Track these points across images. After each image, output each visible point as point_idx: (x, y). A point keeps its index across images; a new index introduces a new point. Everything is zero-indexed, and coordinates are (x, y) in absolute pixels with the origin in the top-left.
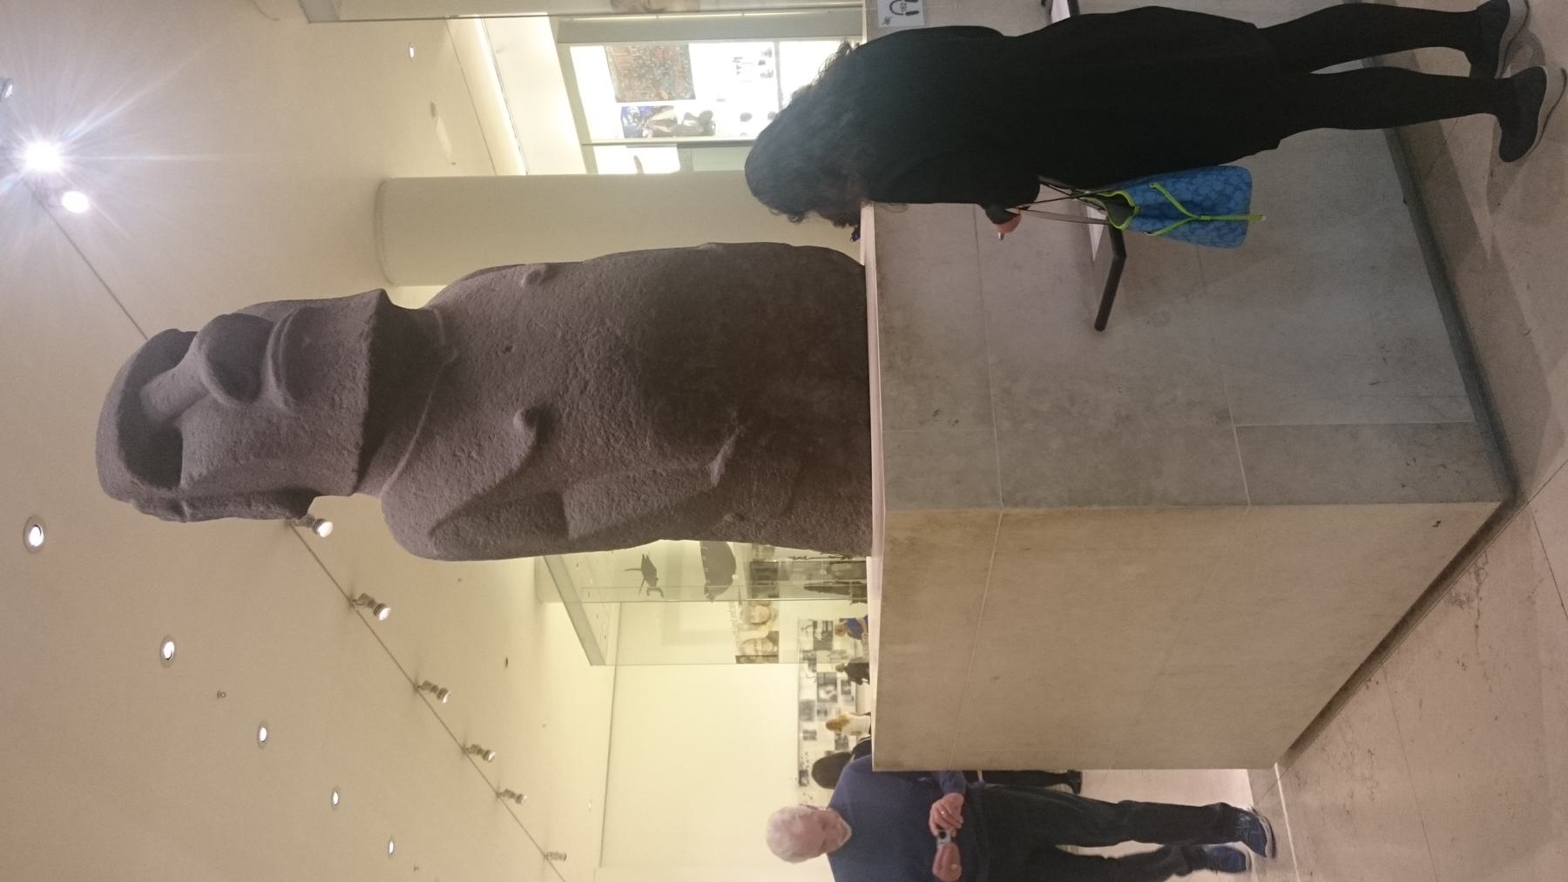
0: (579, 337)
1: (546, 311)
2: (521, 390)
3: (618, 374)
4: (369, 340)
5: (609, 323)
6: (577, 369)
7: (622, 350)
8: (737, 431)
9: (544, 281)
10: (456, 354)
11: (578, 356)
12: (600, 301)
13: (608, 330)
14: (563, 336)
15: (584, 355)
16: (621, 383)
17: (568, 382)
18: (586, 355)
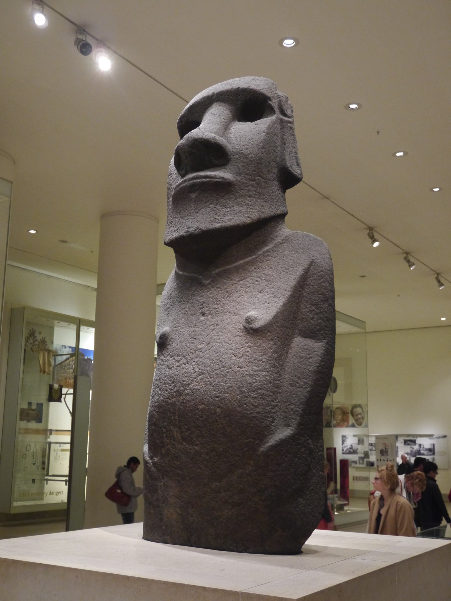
0: (196, 360)
1: (222, 334)
2: (179, 328)
3: (170, 387)
4: (185, 234)
5: (198, 378)
6: (178, 361)
7: (182, 388)
8: (150, 461)
9: (245, 328)
10: (206, 282)
11: (185, 361)
12: (216, 370)
13: (195, 378)
14: (199, 349)
15: (185, 364)
16: (167, 390)
17: (174, 357)
18: (184, 366)
